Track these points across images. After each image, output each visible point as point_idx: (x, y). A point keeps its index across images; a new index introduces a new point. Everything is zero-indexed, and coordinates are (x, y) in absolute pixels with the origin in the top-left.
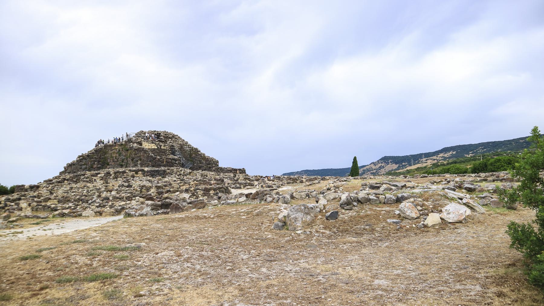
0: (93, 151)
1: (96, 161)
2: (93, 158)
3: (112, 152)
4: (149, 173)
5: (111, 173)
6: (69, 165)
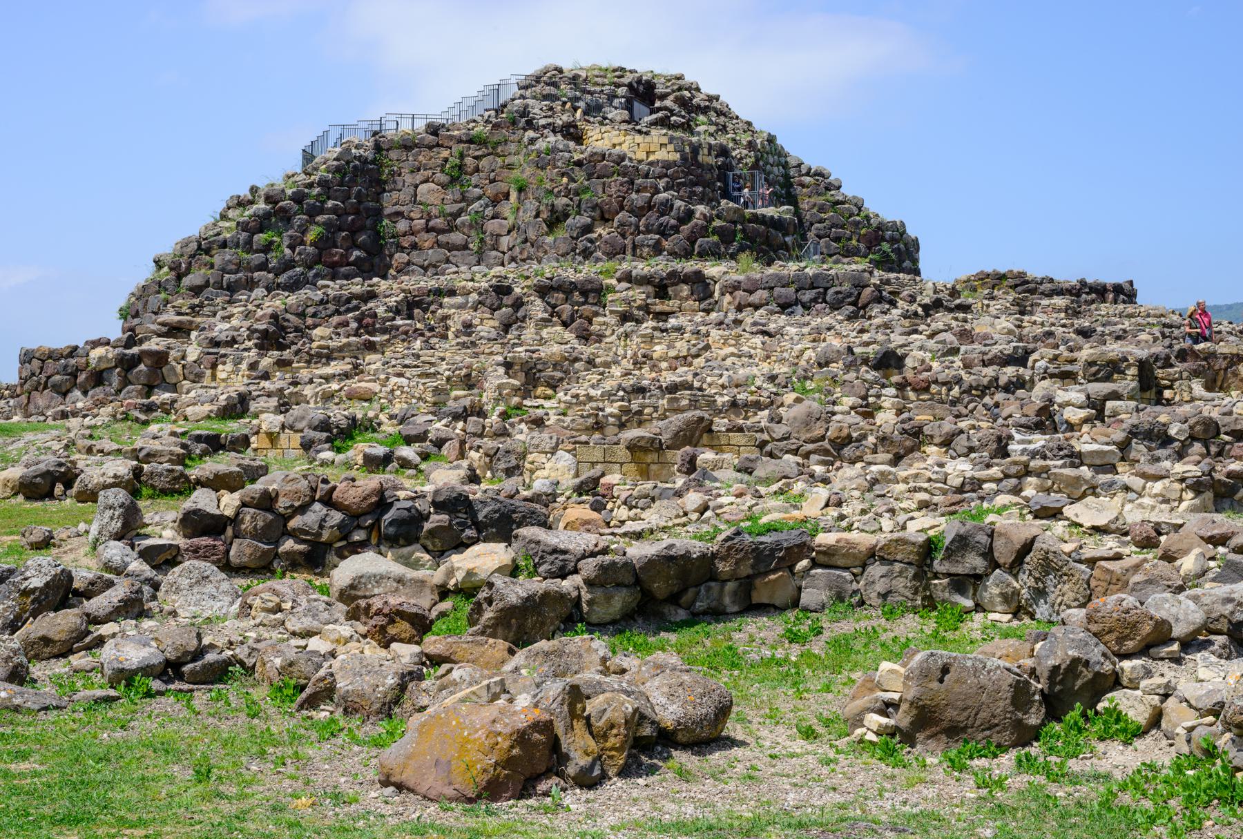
1: (341, 229)
2: (322, 211)
3: (419, 177)
4: (761, 295)
5: (517, 290)
6: (194, 246)
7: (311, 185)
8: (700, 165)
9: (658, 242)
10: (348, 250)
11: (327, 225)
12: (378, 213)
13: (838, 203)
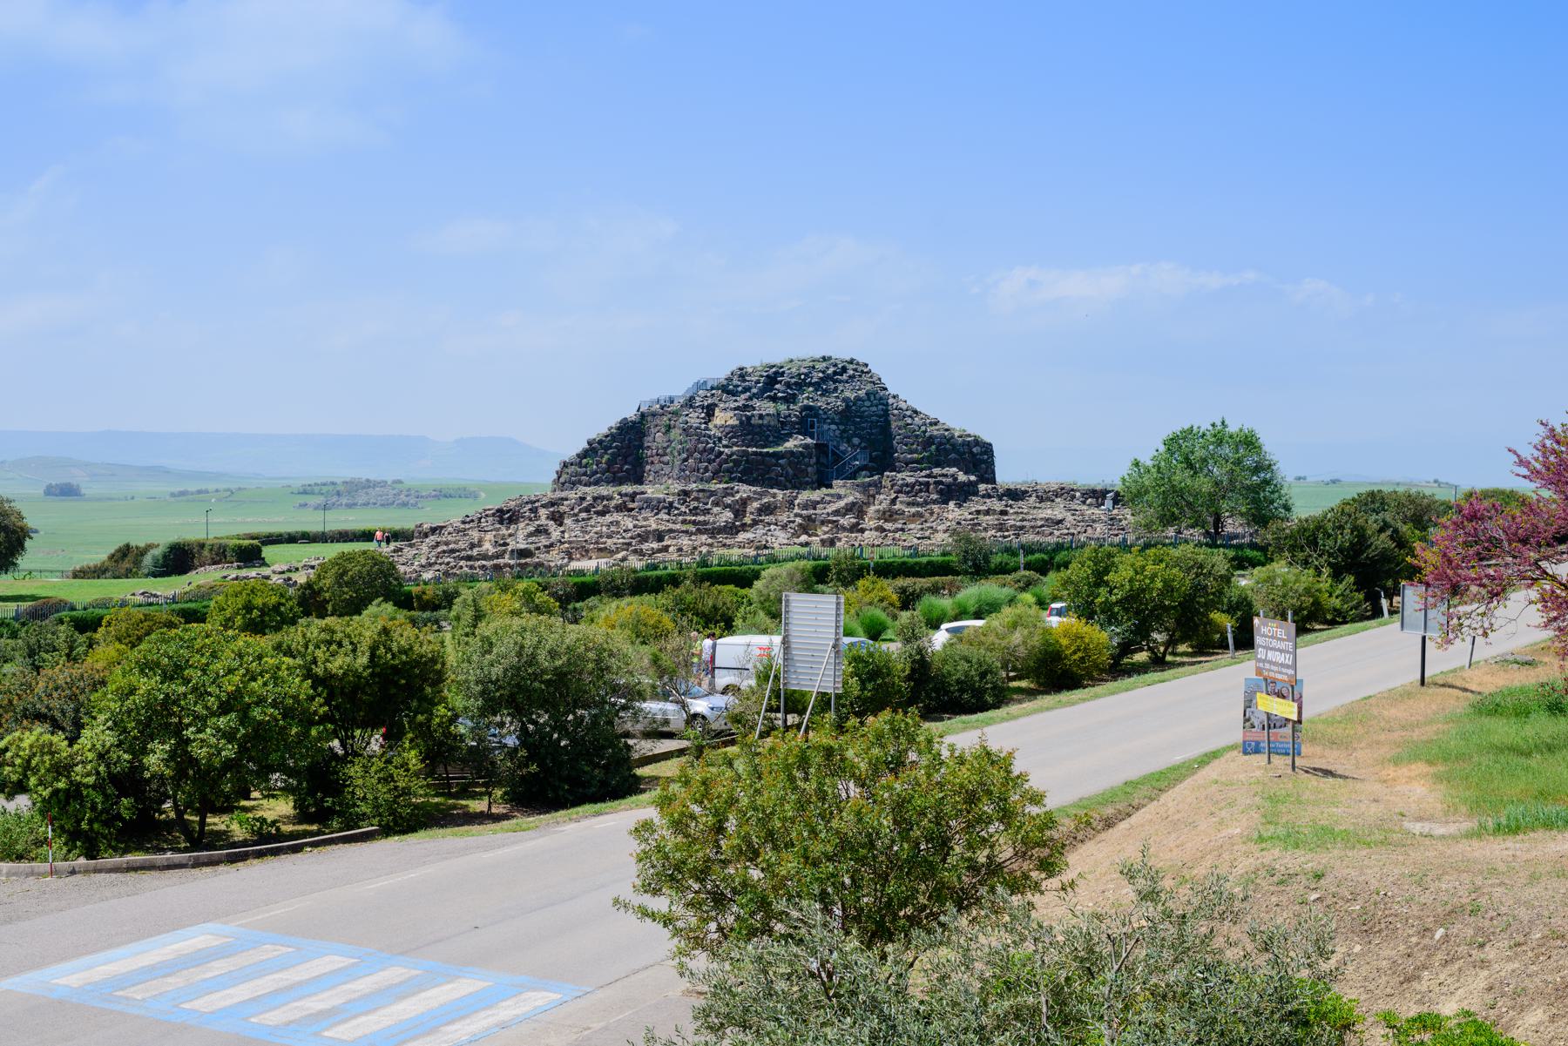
0: (614, 431)
7: (607, 436)
8: (753, 426)
9: (707, 467)
10: (622, 466)
11: (612, 454)
12: (641, 446)
13: (908, 424)
